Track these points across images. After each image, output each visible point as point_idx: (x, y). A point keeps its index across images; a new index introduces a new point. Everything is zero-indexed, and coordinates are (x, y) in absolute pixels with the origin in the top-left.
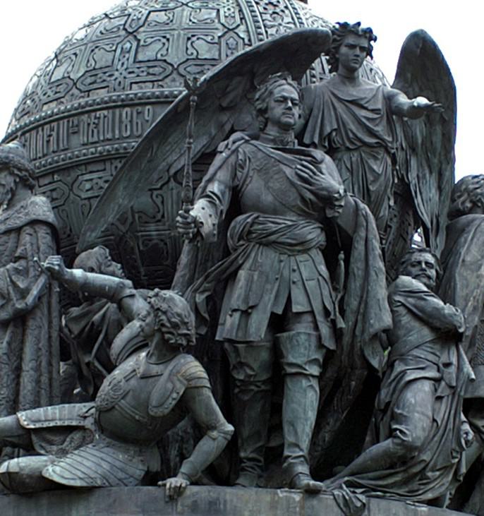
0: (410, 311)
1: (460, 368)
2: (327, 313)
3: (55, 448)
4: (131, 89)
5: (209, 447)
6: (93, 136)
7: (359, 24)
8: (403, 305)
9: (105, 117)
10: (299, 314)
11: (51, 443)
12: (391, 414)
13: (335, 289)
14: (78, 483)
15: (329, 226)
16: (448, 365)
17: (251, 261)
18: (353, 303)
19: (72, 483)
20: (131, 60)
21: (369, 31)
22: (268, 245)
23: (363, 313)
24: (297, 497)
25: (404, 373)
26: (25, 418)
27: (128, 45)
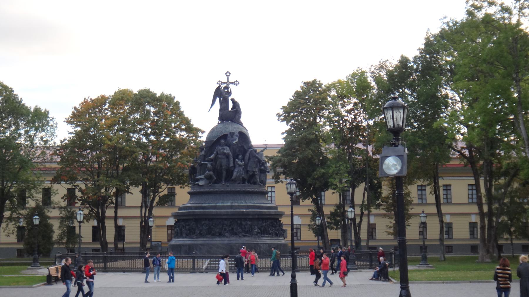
5: (213, 180)
24: (222, 185)
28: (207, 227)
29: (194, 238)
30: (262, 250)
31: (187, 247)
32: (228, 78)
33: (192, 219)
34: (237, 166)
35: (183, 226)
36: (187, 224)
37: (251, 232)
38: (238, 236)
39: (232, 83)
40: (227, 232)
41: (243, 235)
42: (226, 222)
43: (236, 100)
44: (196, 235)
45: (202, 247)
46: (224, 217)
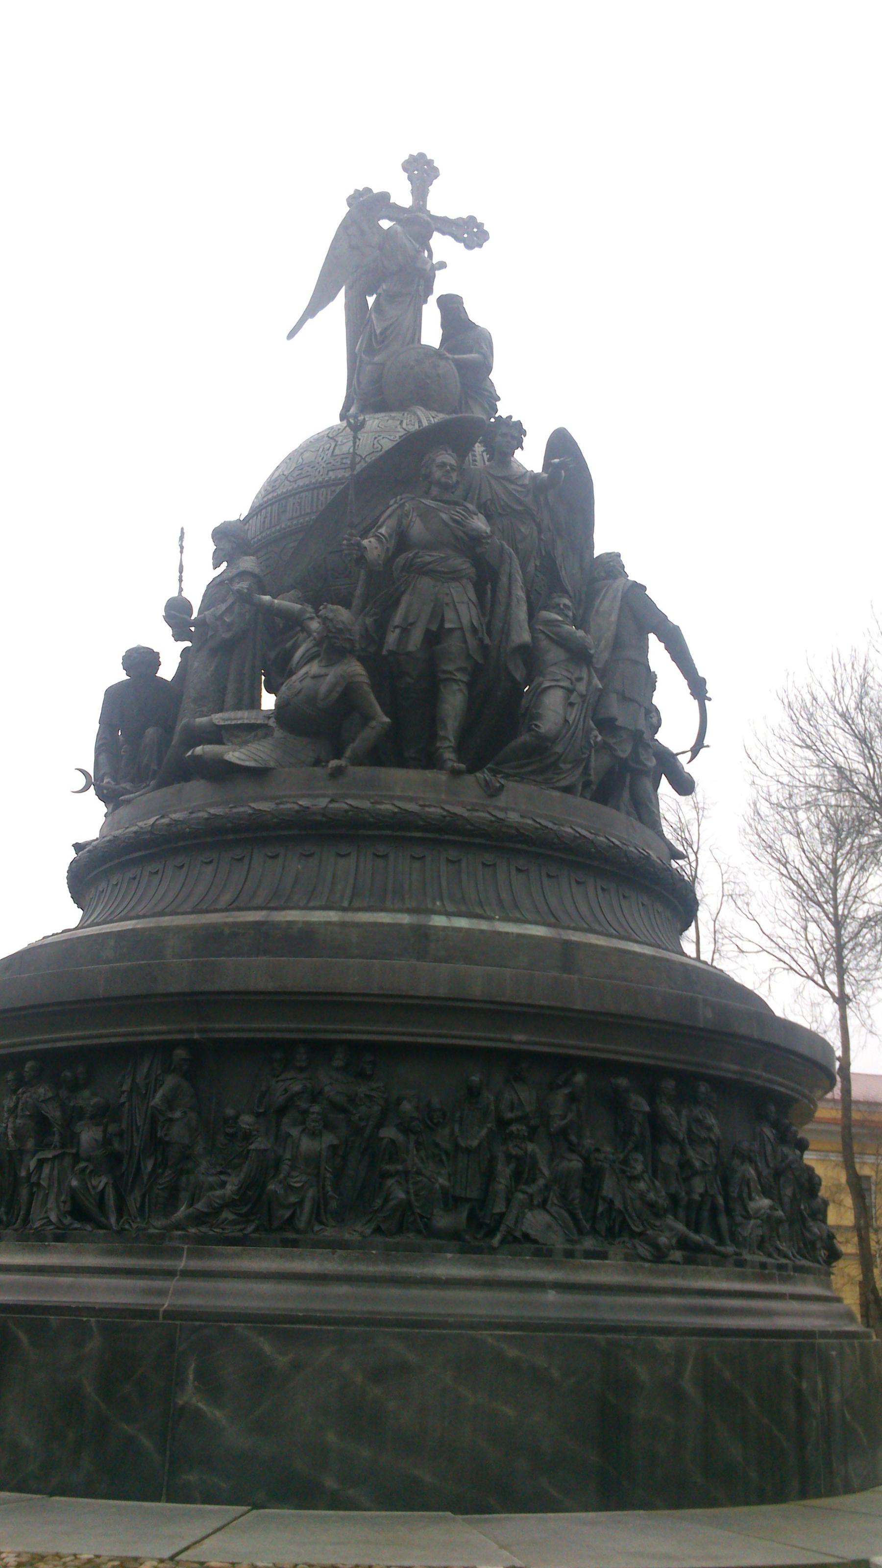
0: (548, 636)
1: (589, 683)
2: (474, 630)
3: (239, 740)
4: (327, 474)
6: (296, 512)
7: (510, 417)
8: (543, 632)
9: (306, 497)
10: (451, 630)
11: (236, 737)
12: (533, 716)
13: (484, 615)
14: (252, 764)
15: (479, 562)
16: (579, 679)
17: (411, 587)
18: (498, 625)
19: (247, 764)
20: (329, 455)
21: (519, 423)
22: (425, 573)
23: (506, 633)
25: (542, 683)
26: (218, 718)
27: (328, 446)
28: (329, 1139)
29: (176, 1253)
30: (836, 1397)
31: (94, 1344)
32: (420, 191)
33: (165, 1048)
34: (554, 654)
35: (42, 1124)
36: (87, 1099)
37: (723, 1220)
38: (643, 1250)
39: (448, 226)
40: (543, 1205)
41: (683, 1244)
42: (526, 1095)
43: (475, 313)
44: (199, 1219)
45: (282, 1361)
46: (520, 1038)
